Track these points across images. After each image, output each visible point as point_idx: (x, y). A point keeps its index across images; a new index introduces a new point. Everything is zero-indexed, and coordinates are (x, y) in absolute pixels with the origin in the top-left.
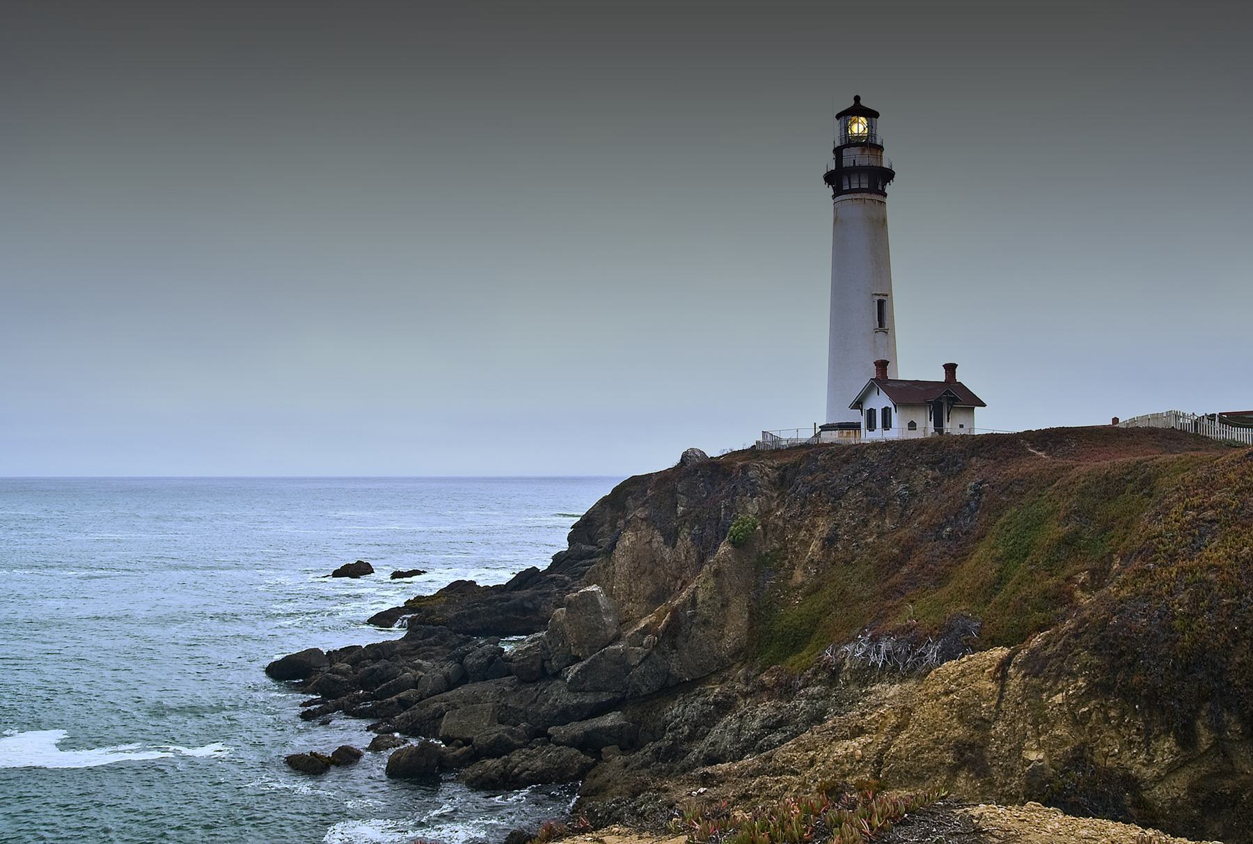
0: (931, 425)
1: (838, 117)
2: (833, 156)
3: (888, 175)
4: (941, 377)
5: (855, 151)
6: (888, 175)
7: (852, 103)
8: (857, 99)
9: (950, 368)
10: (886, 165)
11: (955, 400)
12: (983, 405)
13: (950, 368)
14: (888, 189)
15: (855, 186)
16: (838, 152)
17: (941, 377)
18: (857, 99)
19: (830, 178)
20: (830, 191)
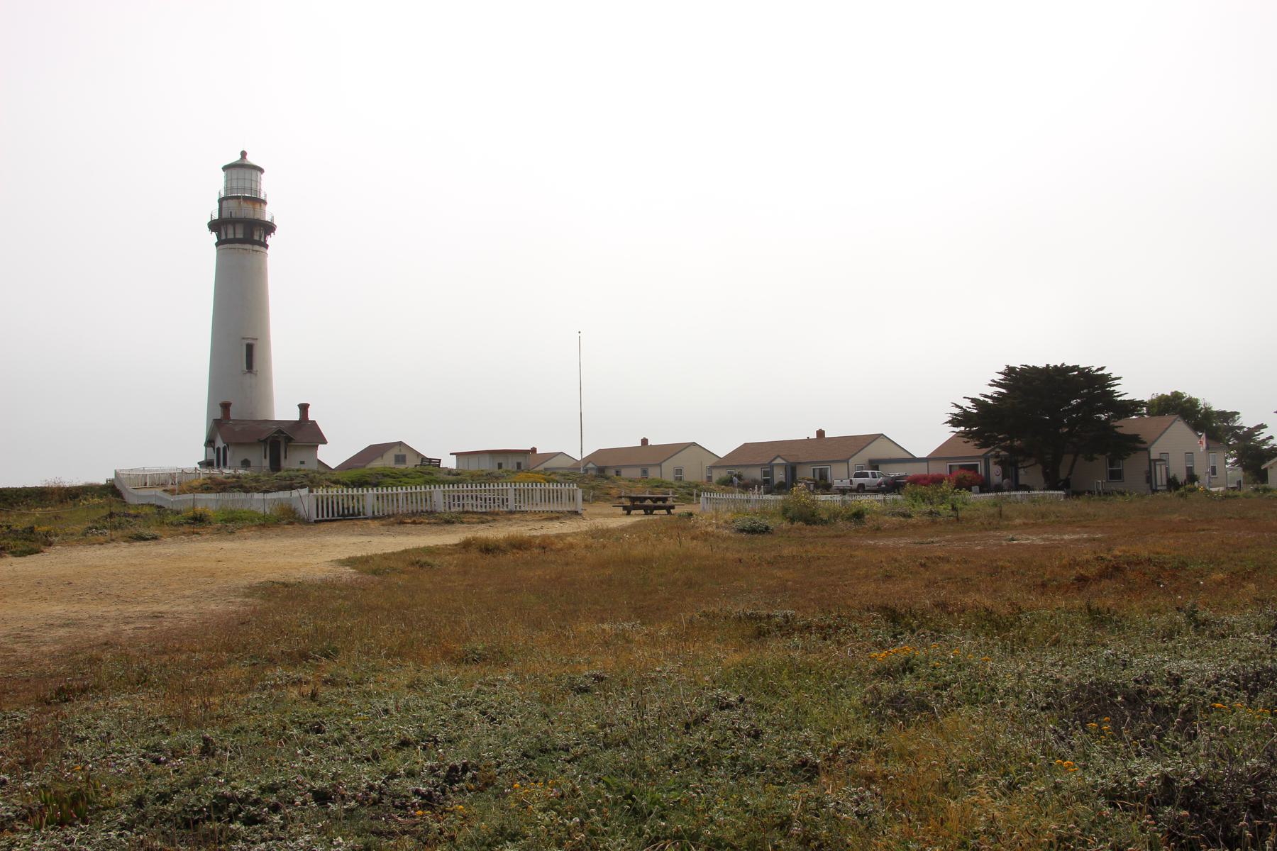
0: (266, 463)
1: (225, 168)
2: (217, 206)
3: (269, 228)
4: (295, 416)
5: (233, 203)
6: (269, 228)
7: (236, 158)
8: (244, 154)
9: (304, 408)
10: (268, 218)
11: (289, 439)
12: (324, 442)
13: (304, 408)
14: (270, 240)
15: (231, 236)
16: (221, 201)
17: (295, 416)
18: (244, 154)
19: (214, 226)
20: (213, 238)
